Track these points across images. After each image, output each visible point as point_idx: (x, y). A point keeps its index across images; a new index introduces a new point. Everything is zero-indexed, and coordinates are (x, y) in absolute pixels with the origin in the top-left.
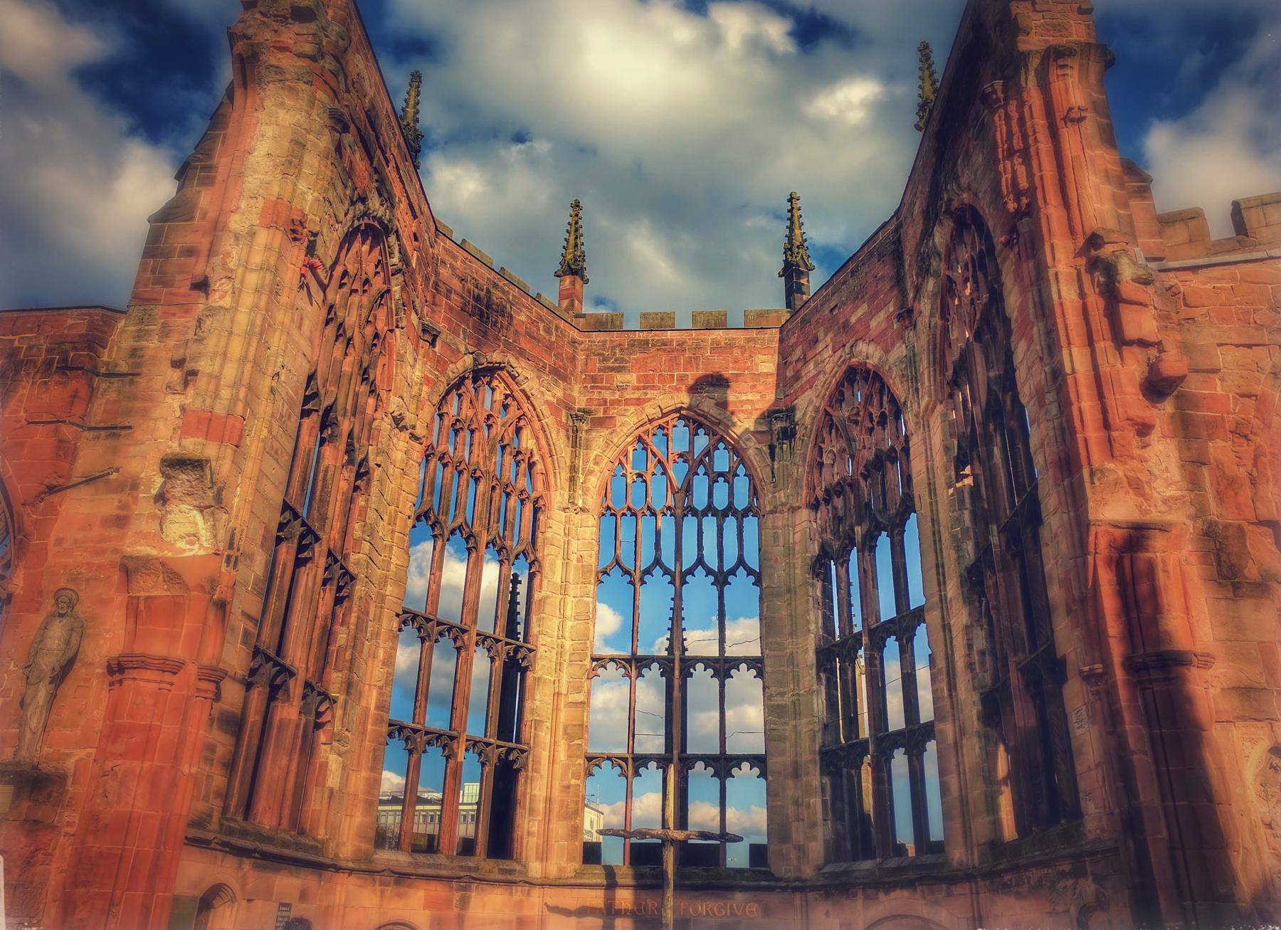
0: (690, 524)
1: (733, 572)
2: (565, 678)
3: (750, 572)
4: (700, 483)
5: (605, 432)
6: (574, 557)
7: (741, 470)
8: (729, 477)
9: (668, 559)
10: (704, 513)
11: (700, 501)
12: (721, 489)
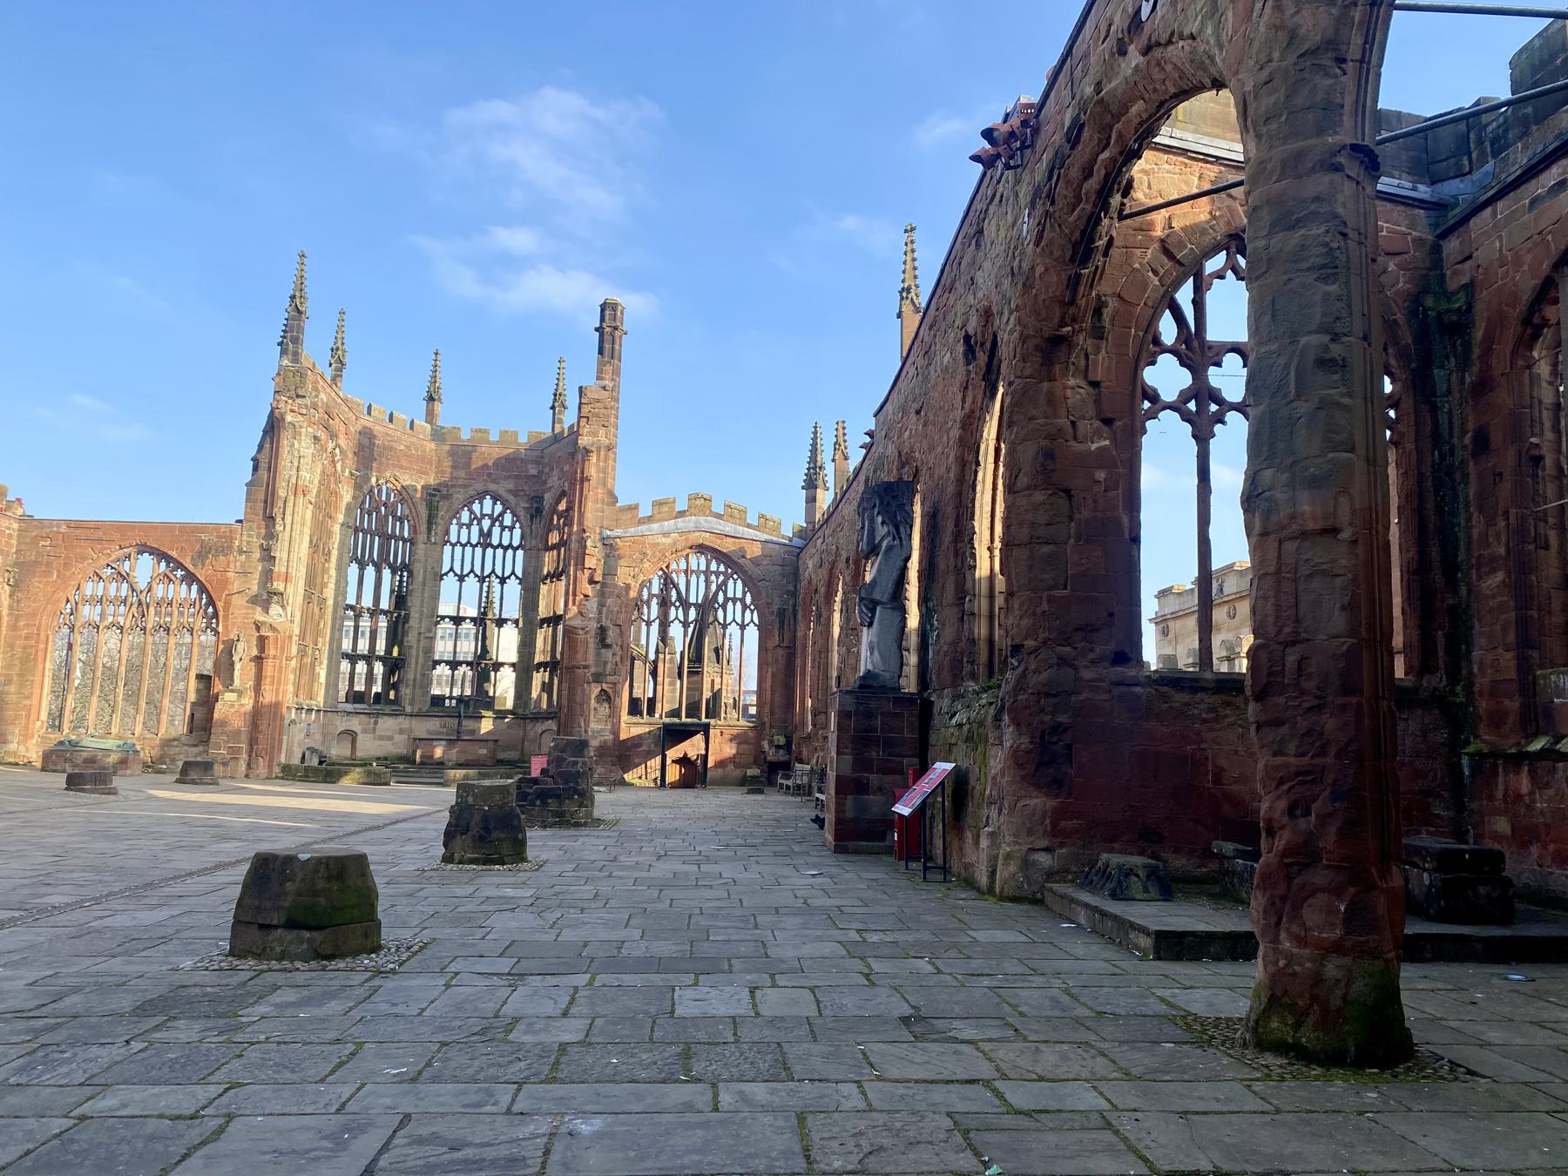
0: (489, 551)
1: (509, 577)
2: (423, 626)
3: (517, 578)
4: (496, 530)
5: (447, 503)
6: (429, 567)
7: (517, 525)
8: (511, 528)
9: (478, 570)
10: (497, 547)
11: (495, 542)
12: (507, 533)
